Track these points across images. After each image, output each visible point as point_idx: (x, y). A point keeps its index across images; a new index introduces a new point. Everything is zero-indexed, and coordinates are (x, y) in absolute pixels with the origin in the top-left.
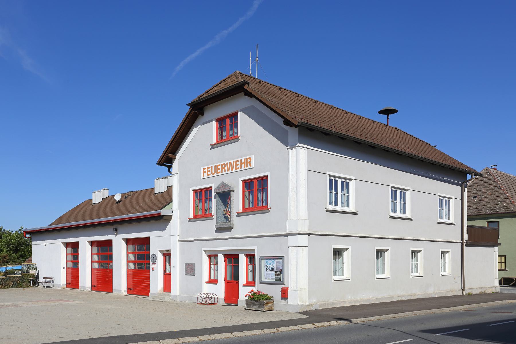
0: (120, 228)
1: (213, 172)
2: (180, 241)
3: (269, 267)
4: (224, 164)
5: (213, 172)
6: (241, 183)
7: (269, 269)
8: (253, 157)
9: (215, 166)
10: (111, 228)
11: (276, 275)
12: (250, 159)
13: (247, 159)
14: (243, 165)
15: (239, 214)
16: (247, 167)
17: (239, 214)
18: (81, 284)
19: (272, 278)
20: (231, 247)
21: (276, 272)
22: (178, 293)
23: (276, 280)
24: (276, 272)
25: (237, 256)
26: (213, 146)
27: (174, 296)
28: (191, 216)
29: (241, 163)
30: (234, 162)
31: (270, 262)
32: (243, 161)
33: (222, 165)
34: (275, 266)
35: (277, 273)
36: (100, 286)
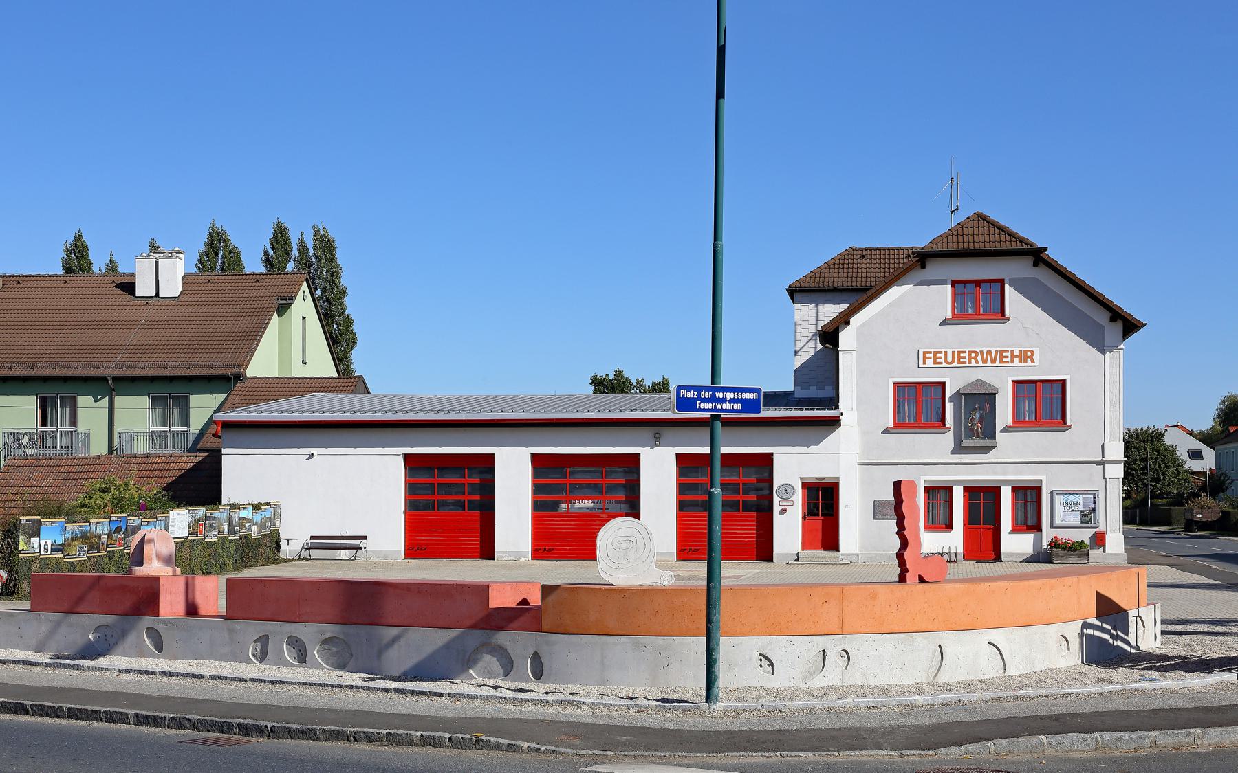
0: (668, 432)
1: (950, 359)
2: (860, 464)
3: (1069, 505)
4: (976, 353)
5: (950, 359)
6: (1010, 386)
7: (1068, 508)
8: (1036, 350)
9: (953, 353)
10: (647, 433)
11: (1082, 515)
12: (1033, 353)
13: (1026, 352)
14: (1016, 360)
15: (1006, 430)
16: (1026, 362)
17: (1006, 430)
18: (500, 545)
19: (1075, 518)
20: (982, 475)
21: (1082, 511)
22: (855, 550)
23: (1082, 522)
24: (1082, 511)
25: (950, 490)
26: (945, 322)
27: (843, 555)
28: (891, 424)
29: (1013, 356)
30: (996, 352)
31: (1072, 498)
32: (1016, 353)
33: (970, 352)
34: (1081, 503)
35: (1085, 513)
36: (568, 548)
